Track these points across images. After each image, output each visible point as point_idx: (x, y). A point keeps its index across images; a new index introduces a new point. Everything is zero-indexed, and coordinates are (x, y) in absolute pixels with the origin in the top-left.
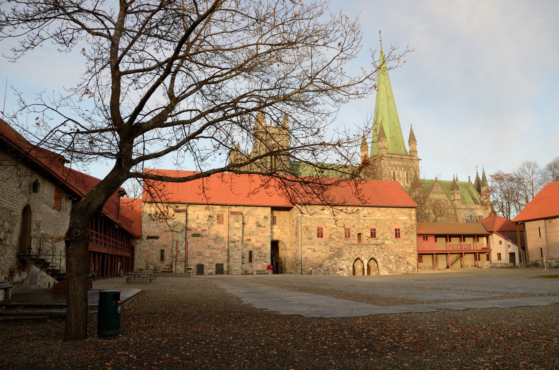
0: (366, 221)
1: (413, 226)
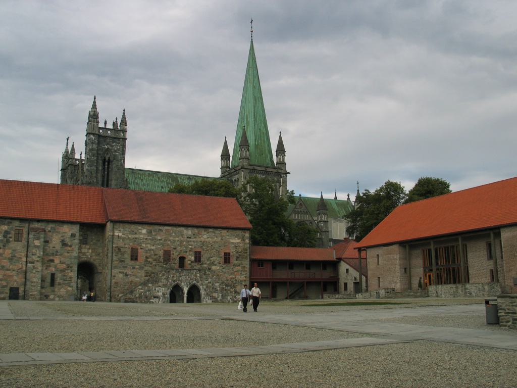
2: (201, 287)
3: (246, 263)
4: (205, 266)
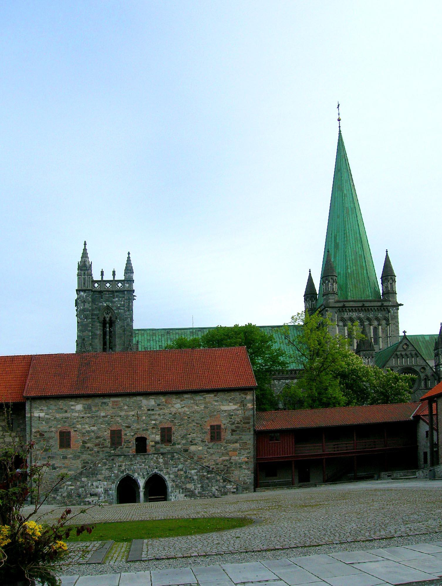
0: (153, 417)
1: (248, 418)
2: (166, 477)
3: (249, 438)
4: (180, 446)
